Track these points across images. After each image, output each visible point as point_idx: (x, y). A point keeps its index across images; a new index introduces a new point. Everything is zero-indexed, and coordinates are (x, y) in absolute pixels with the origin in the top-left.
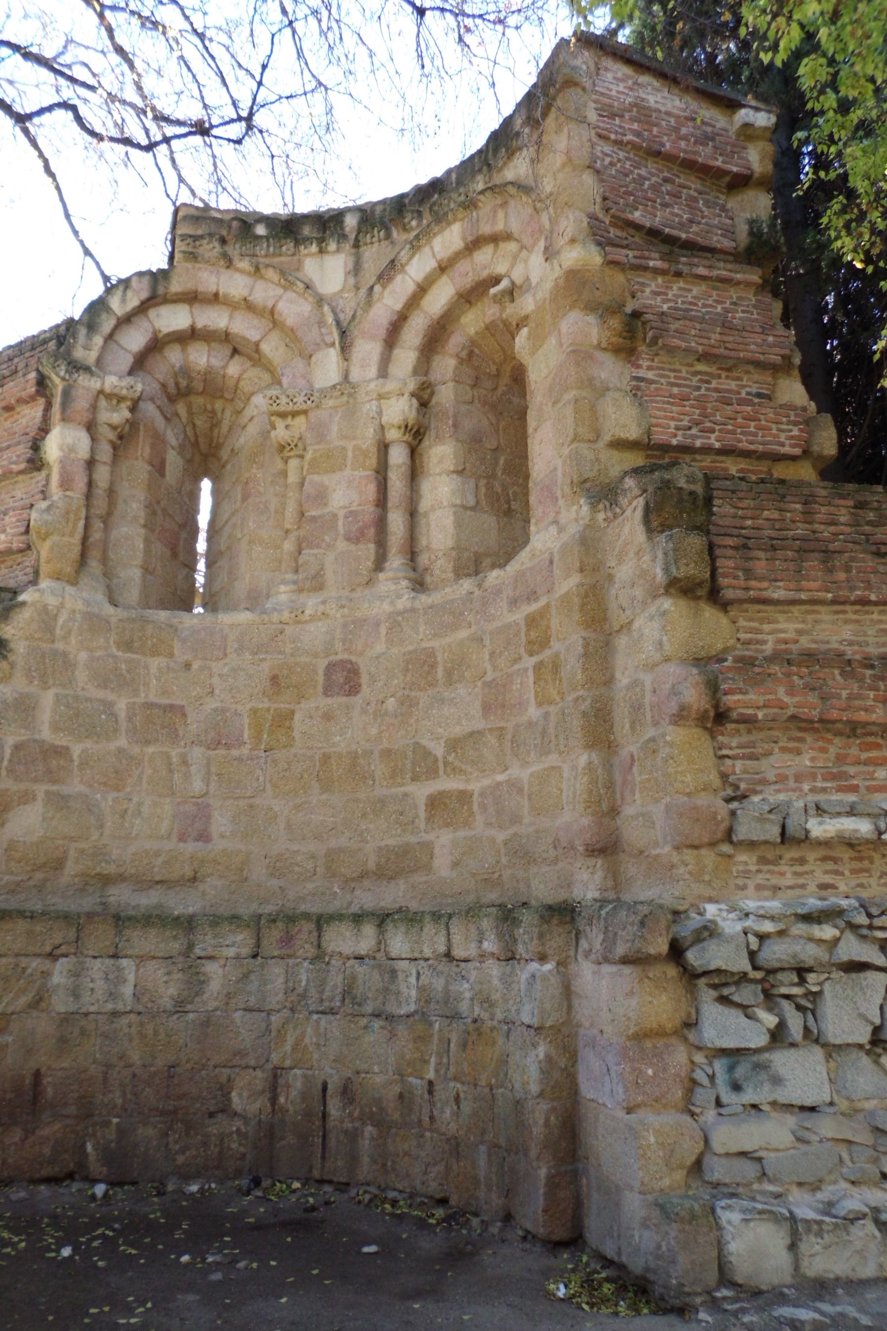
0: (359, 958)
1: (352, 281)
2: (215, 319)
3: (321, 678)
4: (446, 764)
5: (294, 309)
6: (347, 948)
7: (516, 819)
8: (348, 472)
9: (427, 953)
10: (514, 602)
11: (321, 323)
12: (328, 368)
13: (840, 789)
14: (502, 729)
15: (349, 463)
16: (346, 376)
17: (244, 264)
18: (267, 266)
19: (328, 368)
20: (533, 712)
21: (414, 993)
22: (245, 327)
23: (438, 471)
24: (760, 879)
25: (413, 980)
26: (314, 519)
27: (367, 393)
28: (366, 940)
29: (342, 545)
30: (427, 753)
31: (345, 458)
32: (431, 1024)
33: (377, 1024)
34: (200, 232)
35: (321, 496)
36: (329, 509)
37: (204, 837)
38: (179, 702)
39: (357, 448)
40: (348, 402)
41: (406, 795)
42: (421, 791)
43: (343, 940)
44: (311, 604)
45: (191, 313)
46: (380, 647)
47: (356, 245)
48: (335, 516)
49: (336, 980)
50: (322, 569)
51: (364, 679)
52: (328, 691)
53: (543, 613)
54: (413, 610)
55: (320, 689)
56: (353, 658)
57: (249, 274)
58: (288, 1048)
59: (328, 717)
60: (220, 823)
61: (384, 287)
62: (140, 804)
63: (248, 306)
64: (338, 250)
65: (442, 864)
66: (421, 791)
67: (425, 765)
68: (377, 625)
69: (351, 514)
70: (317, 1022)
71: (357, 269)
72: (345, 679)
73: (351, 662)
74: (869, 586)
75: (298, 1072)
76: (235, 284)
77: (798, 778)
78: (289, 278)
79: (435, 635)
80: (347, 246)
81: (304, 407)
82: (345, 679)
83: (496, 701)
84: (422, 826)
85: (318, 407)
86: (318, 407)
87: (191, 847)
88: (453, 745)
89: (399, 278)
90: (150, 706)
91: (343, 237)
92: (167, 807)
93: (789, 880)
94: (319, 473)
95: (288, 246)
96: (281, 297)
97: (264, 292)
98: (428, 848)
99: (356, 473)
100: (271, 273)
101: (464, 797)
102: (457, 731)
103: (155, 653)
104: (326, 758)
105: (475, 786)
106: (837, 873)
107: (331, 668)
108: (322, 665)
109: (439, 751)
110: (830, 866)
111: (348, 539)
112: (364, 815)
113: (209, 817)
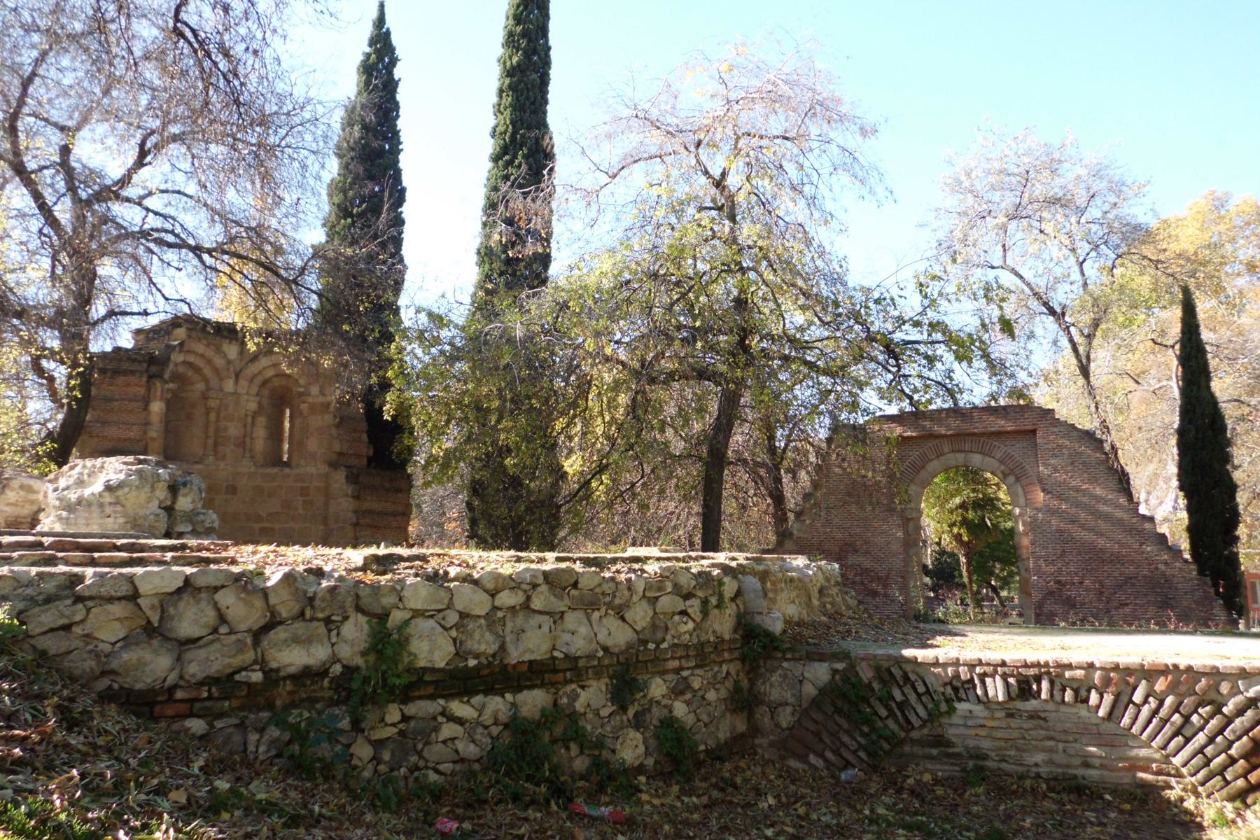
2: (191, 358)
5: (219, 362)
10: (295, 481)
12: (229, 386)
19: (229, 386)
20: (300, 511)
22: (199, 362)
35: (226, 429)
42: (257, 526)
44: (222, 465)
52: (226, 493)
63: (202, 356)
66: (257, 526)
67: (259, 519)
72: (232, 490)
76: (200, 348)
78: (219, 350)
88: (270, 514)
97: (210, 353)
101: (272, 529)
105: (277, 526)
107: (227, 487)
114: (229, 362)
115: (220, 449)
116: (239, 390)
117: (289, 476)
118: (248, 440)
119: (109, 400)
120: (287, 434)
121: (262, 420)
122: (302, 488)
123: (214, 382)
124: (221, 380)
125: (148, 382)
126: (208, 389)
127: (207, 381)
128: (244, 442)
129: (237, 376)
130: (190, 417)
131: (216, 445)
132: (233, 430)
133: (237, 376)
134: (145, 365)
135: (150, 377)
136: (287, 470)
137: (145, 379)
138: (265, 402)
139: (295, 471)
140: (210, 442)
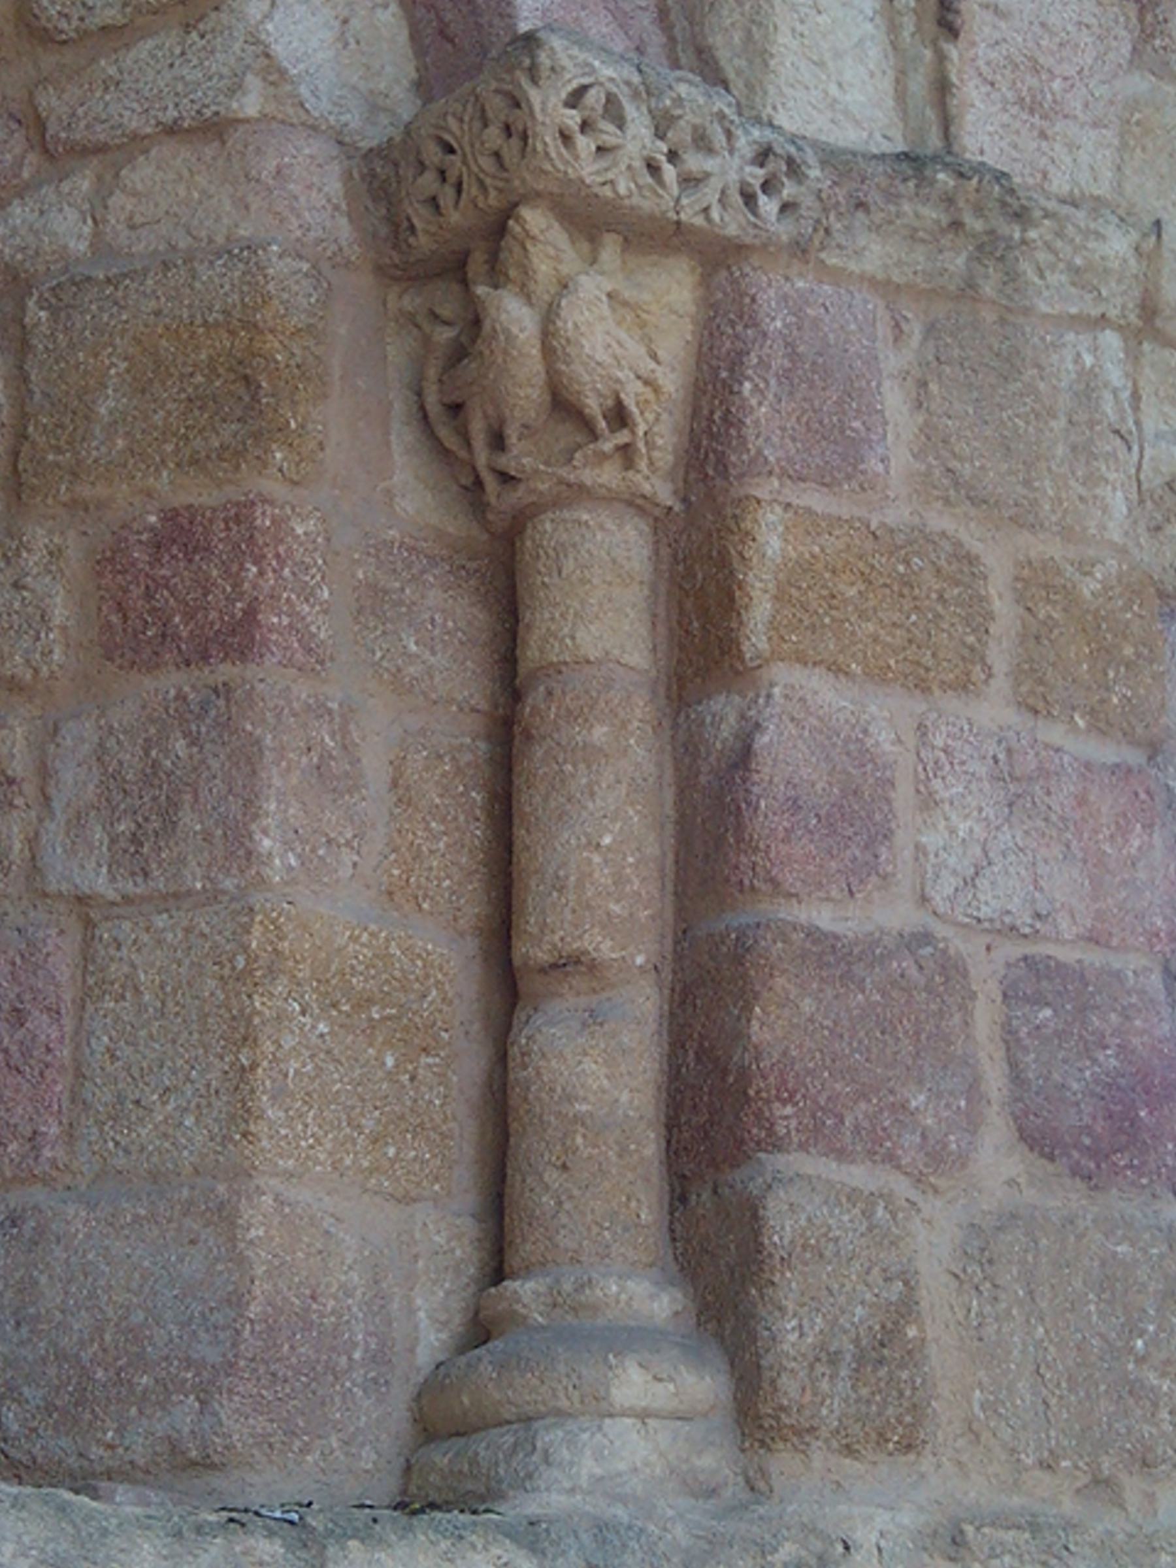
15: (1000, 657)
27: (1083, 277)
29: (998, 1163)
31: (978, 616)
35: (857, 822)
36: (893, 915)
39: (1035, 582)
40: (969, 289)
48: (951, 969)
50: (906, 1309)
81: (732, 223)
85: (800, 249)
86: (800, 249)
94: (837, 669)
99: (1055, 734)
111: (1037, 1139)
115: (804, 1194)
131: (712, 1120)
140: (603, 1070)
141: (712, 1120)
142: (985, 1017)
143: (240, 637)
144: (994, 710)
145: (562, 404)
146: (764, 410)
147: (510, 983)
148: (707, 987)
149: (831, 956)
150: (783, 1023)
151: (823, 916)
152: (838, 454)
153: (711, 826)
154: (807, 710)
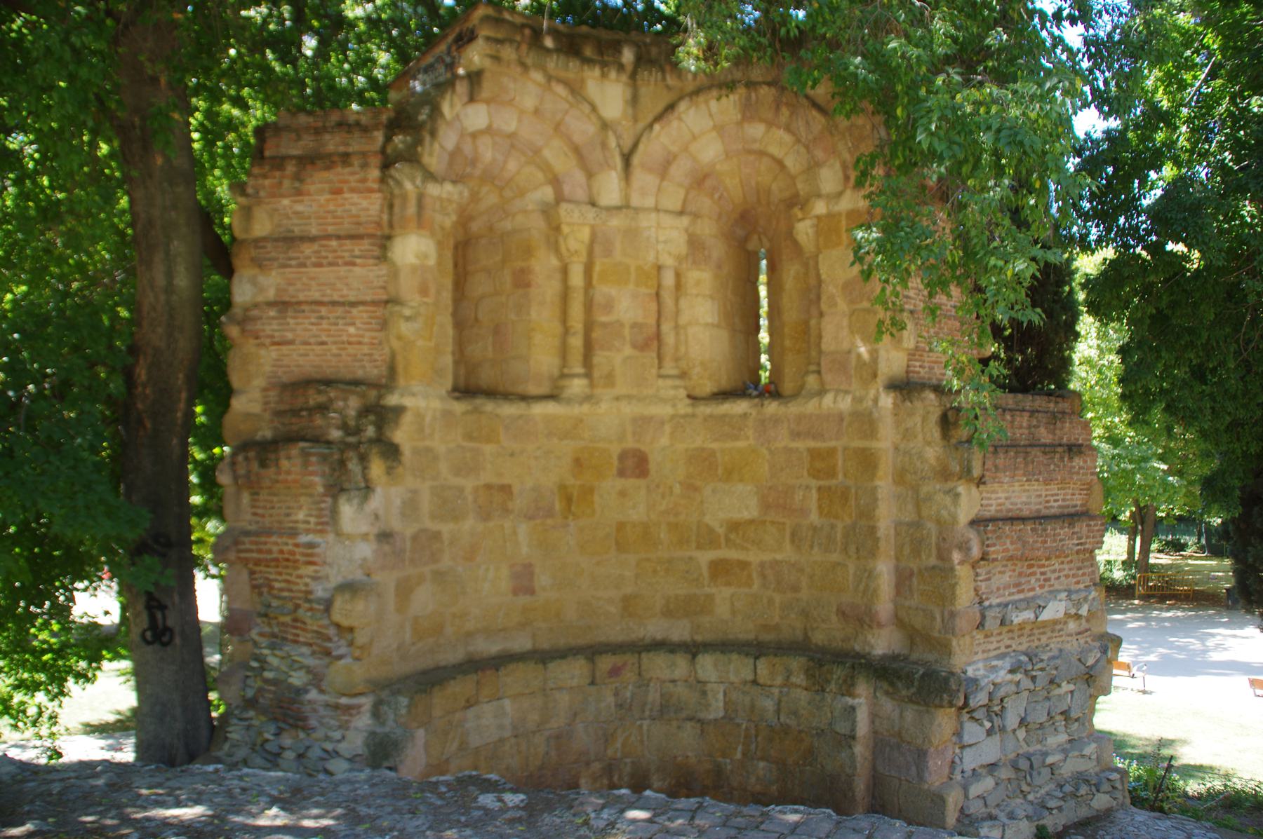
0: (673, 681)
1: (630, 111)
3: (615, 462)
4: (728, 540)
6: (666, 674)
7: (795, 589)
8: (631, 286)
9: (732, 678)
10: (796, 435)
11: (604, 145)
13: (1019, 592)
14: (784, 524)
16: (627, 197)
17: (538, 76)
18: (560, 81)
19: (610, 188)
20: (814, 517)
21: (721, 704)
23: (694, 291)
24: (983, 647)
25: (721, 696)
26: (604, 325)
28: (680, 666)
29: (628, 351)
30: (711, 531)
32: (739, 725)
33: (689, 725)
34: (500, 36)
35: (609, 306)
37: (532, 592)
38: (506, 481)
41: (691, 558)
42: (705, 557)
43: (661, 667)
45: (489, 112)
46: (664, 441)
47: (633, 76)
48: (622, 325)
49: (653, 696)
51: (652, 466)
52: (622, 473)
53: (832, 452)
54: (694, 415)
55: (614, 471)
56: (643, 448)
57: (539, 85)
58: (619, 745)
59: (623, 494)
60: (543, 579)
61: (662, 128)
62: (487, 569)
64: (618, 81)
65: (722, 609)
67: (708, 539)
68: (663, 423)
69: (634, 325)
70: (641, 726)
71: (634, 100)
72: (636, 464)
73: (640, 451)
74: (1040, 473)
75: (628, 760)
77: (1005, 588)
79: (716, 440)
80: (624, 78)
82: (636, 464)
83: (776, 501)
84: (706, 583)
87: (523, 600)
88: (734, 526)
89: (675, 124)
90: (489, 487)
91: (621, 67)
92: (505, 572)
93: (995, 645)
95: (574, 64)
96: (567, 112)
98: (710, 597)
100: (560, 90)
101: (744, 565)
102: (736, 516)
103: (488, 440)
104: (621, 526)
106: (1013, 638)
107: (623, 456)
108: (615, 449)
109: (721, 531)
110: (1010, 635)
111: (634, 346)
112: (655, 572)
113: (532, 574)
114: (605, 125)
116: (635, 201)
117: (776, 420)
118: (666, 327)
119: (290, 240)
120: (764, 310)
121: (702, 279)
122: (814, 454)
123: (575, 182)
124: (590, 175)
125: (382, 180)
126: (560, 198)
127: (555, 182)
128: (658, 336)
129: (627, 159)
130: (522, 280)
131: (588, 348)
132: (627, 306)
133: (627, 159)
134: (379, 136)
135: (386, 165)
136: (772, 407)
137: (375, 173)
138: (707, 229)
139: (793, 409)
140: (576, 342)
141: (588, 348)
142: (627, 332)
143: (528, 285)
144: (631, 286)
145: (568, 250)
146: (598, 249)
147: (566, 331)
148: (589, 327)
149: (604, 325)
150: (597, 334)
151: (604, 319)
152: (608, 252)
153: (589, 306)
154: (602, 290)
